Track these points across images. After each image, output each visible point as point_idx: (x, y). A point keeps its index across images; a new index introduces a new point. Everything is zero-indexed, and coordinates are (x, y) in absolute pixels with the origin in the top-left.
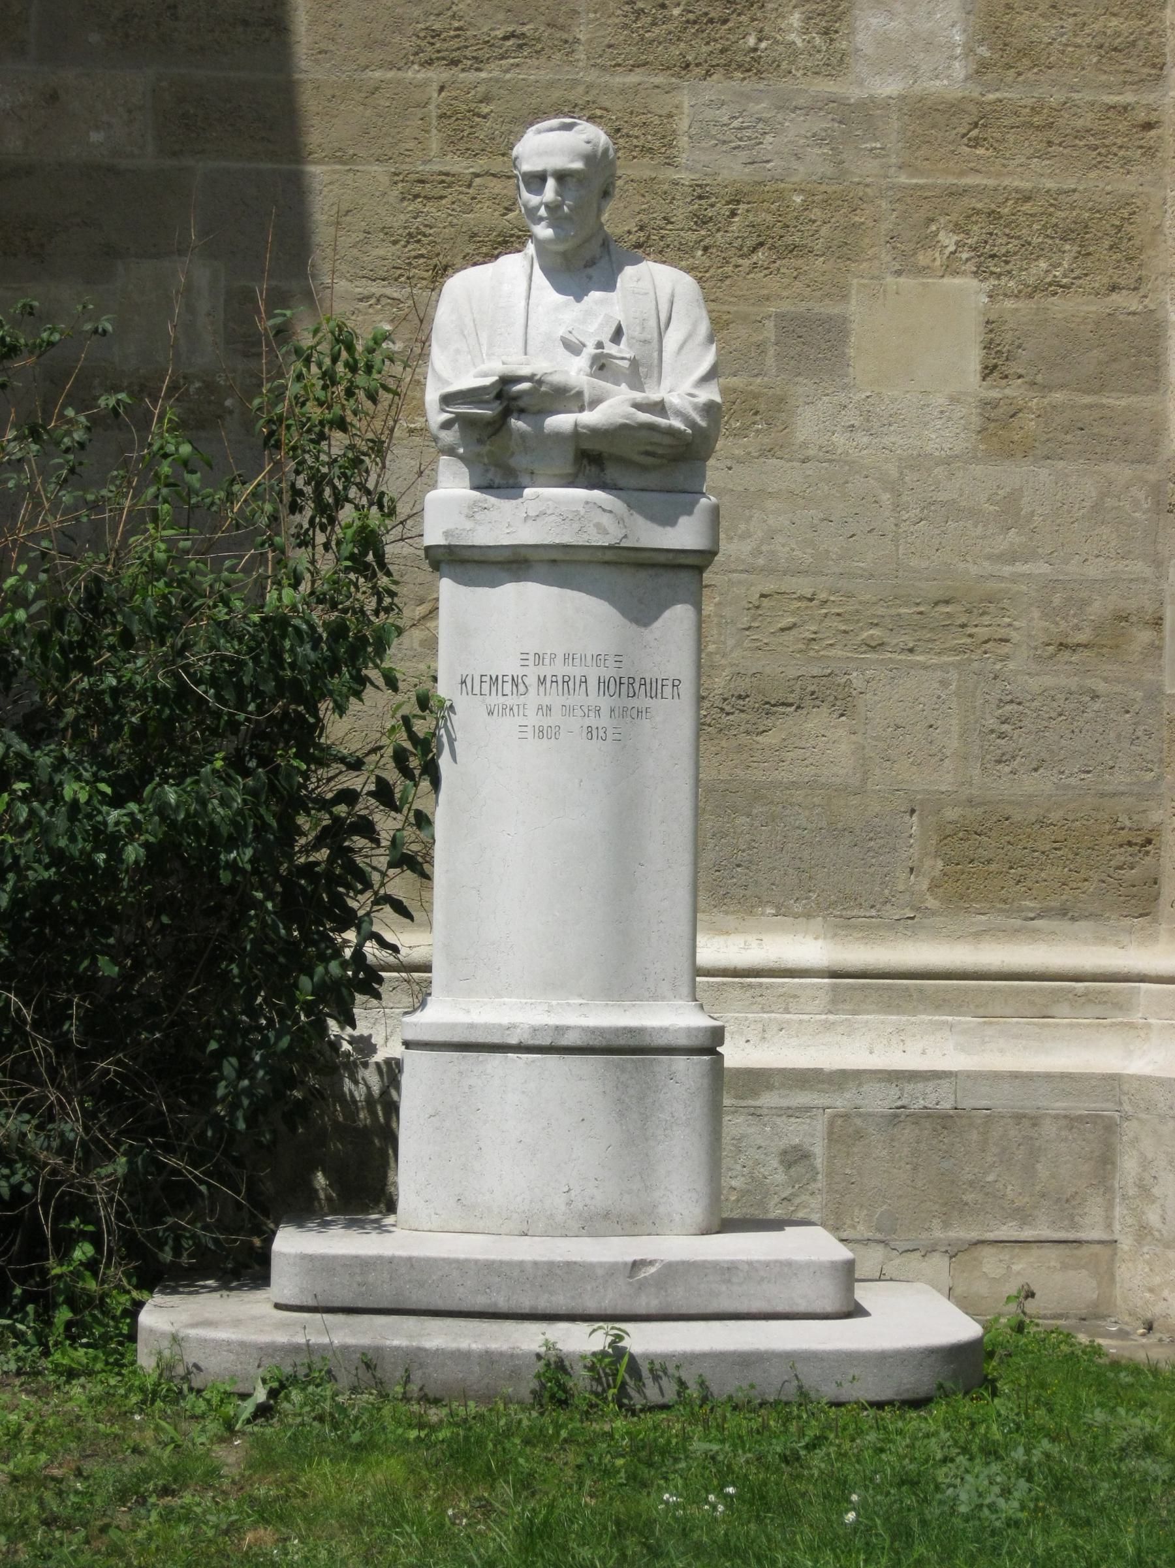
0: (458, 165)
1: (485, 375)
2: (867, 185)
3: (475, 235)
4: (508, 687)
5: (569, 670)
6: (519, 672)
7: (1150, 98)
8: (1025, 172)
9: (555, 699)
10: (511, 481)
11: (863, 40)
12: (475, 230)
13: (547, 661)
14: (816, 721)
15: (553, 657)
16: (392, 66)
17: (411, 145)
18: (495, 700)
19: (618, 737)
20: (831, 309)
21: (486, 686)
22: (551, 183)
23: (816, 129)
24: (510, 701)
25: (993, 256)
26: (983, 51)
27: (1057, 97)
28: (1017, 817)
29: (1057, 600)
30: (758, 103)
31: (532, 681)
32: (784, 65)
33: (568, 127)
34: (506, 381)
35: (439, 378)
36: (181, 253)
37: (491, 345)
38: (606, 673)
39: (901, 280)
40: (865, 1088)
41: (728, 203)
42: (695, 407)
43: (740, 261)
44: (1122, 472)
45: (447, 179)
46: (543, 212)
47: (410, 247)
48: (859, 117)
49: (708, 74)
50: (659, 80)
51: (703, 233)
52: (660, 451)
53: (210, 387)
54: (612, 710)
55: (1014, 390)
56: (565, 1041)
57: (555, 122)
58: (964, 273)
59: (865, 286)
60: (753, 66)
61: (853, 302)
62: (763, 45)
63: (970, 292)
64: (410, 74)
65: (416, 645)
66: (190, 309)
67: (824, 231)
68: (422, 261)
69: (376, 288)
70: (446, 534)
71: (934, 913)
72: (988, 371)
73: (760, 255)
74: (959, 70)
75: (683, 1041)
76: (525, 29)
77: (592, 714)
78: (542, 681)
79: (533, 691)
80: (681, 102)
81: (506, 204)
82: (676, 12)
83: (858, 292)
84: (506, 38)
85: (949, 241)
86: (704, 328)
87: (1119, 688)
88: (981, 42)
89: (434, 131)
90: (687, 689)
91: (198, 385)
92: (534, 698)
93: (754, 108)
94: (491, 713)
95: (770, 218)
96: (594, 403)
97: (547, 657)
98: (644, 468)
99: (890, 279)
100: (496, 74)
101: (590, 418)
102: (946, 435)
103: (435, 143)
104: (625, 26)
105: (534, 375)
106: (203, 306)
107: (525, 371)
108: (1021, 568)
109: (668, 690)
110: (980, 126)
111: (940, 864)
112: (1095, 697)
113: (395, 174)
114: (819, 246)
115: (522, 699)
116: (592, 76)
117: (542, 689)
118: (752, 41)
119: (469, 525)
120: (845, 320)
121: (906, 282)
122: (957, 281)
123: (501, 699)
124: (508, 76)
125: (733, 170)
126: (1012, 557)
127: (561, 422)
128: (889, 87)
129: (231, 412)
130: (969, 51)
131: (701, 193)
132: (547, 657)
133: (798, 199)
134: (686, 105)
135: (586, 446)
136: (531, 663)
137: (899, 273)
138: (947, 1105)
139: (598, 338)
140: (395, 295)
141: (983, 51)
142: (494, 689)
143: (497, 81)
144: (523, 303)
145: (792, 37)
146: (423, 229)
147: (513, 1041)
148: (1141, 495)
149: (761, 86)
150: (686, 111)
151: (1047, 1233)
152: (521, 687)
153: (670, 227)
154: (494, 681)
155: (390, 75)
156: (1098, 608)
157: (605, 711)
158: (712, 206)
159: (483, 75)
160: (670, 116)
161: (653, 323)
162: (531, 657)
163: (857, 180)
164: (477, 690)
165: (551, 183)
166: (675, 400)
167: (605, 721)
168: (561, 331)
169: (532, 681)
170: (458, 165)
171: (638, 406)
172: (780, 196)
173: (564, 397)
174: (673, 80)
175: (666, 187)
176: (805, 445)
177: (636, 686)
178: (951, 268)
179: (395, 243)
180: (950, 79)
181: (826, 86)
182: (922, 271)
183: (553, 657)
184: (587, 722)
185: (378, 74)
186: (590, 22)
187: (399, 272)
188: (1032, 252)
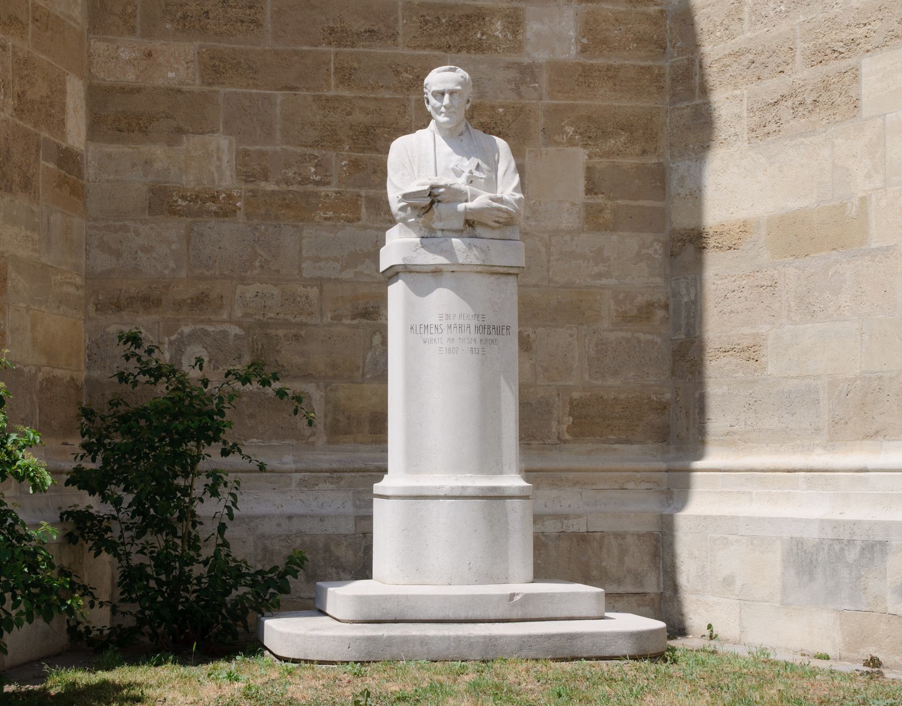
0: (345, 93)
1: (423, 185)
4: (433, 330)
7: (659, 63)
8: (603, 99)
11: (529, 34)
16: (313, 45)
18: (427, 336)
21: (422, 330)
22: (447, 96)
25: (590, 137)
26: (585, 41)
27: (618, 62)
28: (605, 397)
29: (621, 297)
32: (494, 47)
33: (454, 70)
34: (433, 187)
36: (213, 132)
37: (419, 172)
39: (548, 149)
40: (547, 523)
44: (649, 237)
45: (338, 99)
46: (443, 109)
48: (528, 72)
49: (459, 51)
50: (437, 53)
52: (501, 220)
53: (229, 196)
55: (600, 199)
56: (466, 494)
57: (447, 67)
58: (577, 145)
60: (479, 47)
61: (527, 158)
62: (484, 37)
63: (581, 155)
64: (319, 48)
65: (329, 320)
66: (219, 159)
69: (309, 151)
70: (404, 259)
71: (566, 442)
72: (589, 191)
74: (573, 50)
75: (517, 493)
76: (373, 28)
79: (445, 331)
82: (444, 21)
84: (365, 32)
85: (570, 130)
87: (650, 337)
88: (583, 37)
89: (332, 76)
90: (515, 330)
91: (224, 195)
95: (488, 120)
96: (474, 197)
98: (493, 228)
99: (543, 149)
101: (470, 205)
102: (568, 220)
103: (333, 82)
104: (421, 28)
106: (225, 158)
107: (442, 183)
108: (604, 281)
109: (505, 331)
110: (585, 76)
111: (571, 418)
112: (639, 341)
113: (314, 96)
116: (408, 52)
118: (479, 35)
119: (415, 255)
121: (552, 149)
122: (574, 149)
126: (600, 276)
128: (541, 56)
129: (240, 209)
130: (577, 41)
133: (501, 110)
135: (469, 218)
136: (444, 318)
137: (546, 145)
138: (583, 529)
141: (585, 41)
144: (433, 152)
145: (497, 33)
147: (442, 494)
148: (658, 248)
149: (483, 57)
151: (631, 589)
152: (440, 330)
154: (426, 327)
155: (310, 48)
156: (640, 300)
157: (478, 341)
159: (355, 49)
166: (506, 196)
168: (452, 165)
169: (444, 327)
170: (345, 93)
171: (492, 199)
173: (458, 195)
178: (571, 143)
179: (315, 129)
180: (569, 53)
181: (514, 58)
182: (557, 143)
185: (306, 48)
186: (404, 25)
188: (606, 135)
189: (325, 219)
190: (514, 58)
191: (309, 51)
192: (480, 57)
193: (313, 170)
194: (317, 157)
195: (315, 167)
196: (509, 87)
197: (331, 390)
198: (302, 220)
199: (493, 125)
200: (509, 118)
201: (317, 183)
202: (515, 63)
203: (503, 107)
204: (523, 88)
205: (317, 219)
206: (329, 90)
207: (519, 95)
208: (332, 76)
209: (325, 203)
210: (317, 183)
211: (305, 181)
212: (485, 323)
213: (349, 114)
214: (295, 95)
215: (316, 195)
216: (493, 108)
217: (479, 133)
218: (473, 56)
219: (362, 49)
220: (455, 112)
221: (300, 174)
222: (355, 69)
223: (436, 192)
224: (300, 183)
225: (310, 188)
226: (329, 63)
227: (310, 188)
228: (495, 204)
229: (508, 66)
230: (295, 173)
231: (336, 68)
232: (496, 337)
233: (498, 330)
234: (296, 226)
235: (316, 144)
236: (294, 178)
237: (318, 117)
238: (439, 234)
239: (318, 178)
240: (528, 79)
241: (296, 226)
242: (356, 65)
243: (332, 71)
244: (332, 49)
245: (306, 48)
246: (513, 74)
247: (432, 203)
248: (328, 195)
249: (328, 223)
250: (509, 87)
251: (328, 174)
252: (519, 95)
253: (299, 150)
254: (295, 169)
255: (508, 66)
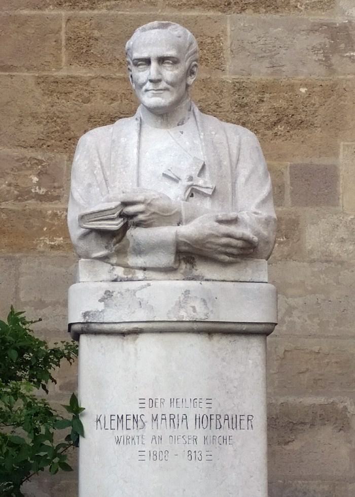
0: (81, 72)
2: (349, 80)
3: (91, 117)
5: (174, 411)
6: (138, 412)
9: (165, 430)
10: (130, 276)
12: (92, 114)
13: (158, 405)
14: (325, 434)
15: (163, 401)
16: (36, 7)
17: (49, 58)
18: (121, 433)
19: (210, 458)
20: (326, 161)
21: (114, 423)
22: (154, 64)
23: (314, 44)
24: (132, 433)
30: (276, 28)
31: (147, 418)
34: (125, 204)
35: (78, 205)
38: (202, 411)
41: (257, 94)
42: (259, 221)
43: (267, 132)
45: (72, 81)
47: (49, 125)
49: (243, 10)
50: (211, 13)
51: (241, 113)
52: (235, 251)
54: (205, 439)
57: (156, 23)
59: (348, 146)
61: (341, 157)
64: (46, 12)
67: (321, 111)
68: (57, 134)
69: (30, 153)
73: (280, 128)
77: (191, 441)
78: (155, 419)
79: (148, 426)
80: (226, 28)
81: (112, 97)
83: (344, 150)
86: (261, 169)
89: (64, 50)
92: (150, 430)
93: (273, 31)
94: (118, 442)
97: (159, 401)
98: (224, 264)
100: (104, 11)
105: (145, 200)
107: (140, 198)
109: (244, 423)
113: (39, 77)
114: (318, 121)
115: (140, 432)
117: (155, 424)
119: (101, 306)
120: (335, 168)
123: (125, 432)
124: (112, 12)
125: (261, 73)
127: (166, 232)
131: (239, 88)
132: (159, 401)
133: (303, 90)
134: (229, 29)
135: (184, 248)
136: (146, 405)
139: (189, 174)
140: (40, 157)
142: (120, 425)
143: (106, 16)
144: (135, 151)
146: (58, 114)
149: (277, 16)
150: (229, 34)
152: (140, 423)
153: (219, 110)
154: (120, 419)
155: (34, 12)
157: (200, 440)
158: (247, 96)
159: (96, 12)
160: (218, 36)
161: (226, 163)
162: (147, 401)
163: (342, 77)
164: (108, 426)
165: (154, 64)
166: (245, 216)
167: (200, 446)
168: (163, 170)
169: (147, 418)
170: (81, 72)
172: (292, 87)
174: (220, 14)
175: (216, 85)
176: (311, 252)
177: (222, 420)
179: (39, 123)
181: (322, 17)
183: (163, 401)
184: (188, 447)
185: (26, 12)
187: (43, 142)
189: (52, 247)
190: (322, 17)
191: (33, 17)
192: (272, 17)
193: (35, 179)
194: (41, 162)
195: (39, 175)
196: (315, 57)
197: (59, 490)
198: (20, 250)
199: (292, 112)
200: (316, 99)
201: (40, 198)
202: (322, 25)
203: (306, 85)
204: (335, 60)
205: (41, 247)
206: (59, 69)
207: (329, 67)
208: (64, 50)
209: (53, 225)
210: (40, 198)
211: (24, 194)
212: (212, 411)
213: (87, 101)
214: (11, 77)
215: (41, 214)
216: (292, 87)
217: (212, 122)
218: (263, 17)
219: (104, 11)
220: (166, 89)
221: (17, 186)
222: (96, 40)
223: (131, 209)
224: (16, 198)
225: (32, 204)
226: (59, 31)
227: (32, 204)
228: (224, 229)
229: (314, 29)
230: (10, 185)
231: (69, 39)
232: (231, 432)
233: (235, 421)
234: (11, 258)
235: (39, 144)
236: (8, 192)
237: (43, 106)
238: (140, 274)
239: (42, 191)
240: (343, 46)
241: (11, 258)
242: (96, 34)
243: (64, 43)
244: (64, 13)
245: (26, 12)
246: (318, 39)
247: (125, 228)
248: (56, 214)
249: (56, 253)
250: (315, 57)
251: (56, 184)
252: (329, 67)
253: (17, 152)
254: (9, 179)
255: (314, 29)
